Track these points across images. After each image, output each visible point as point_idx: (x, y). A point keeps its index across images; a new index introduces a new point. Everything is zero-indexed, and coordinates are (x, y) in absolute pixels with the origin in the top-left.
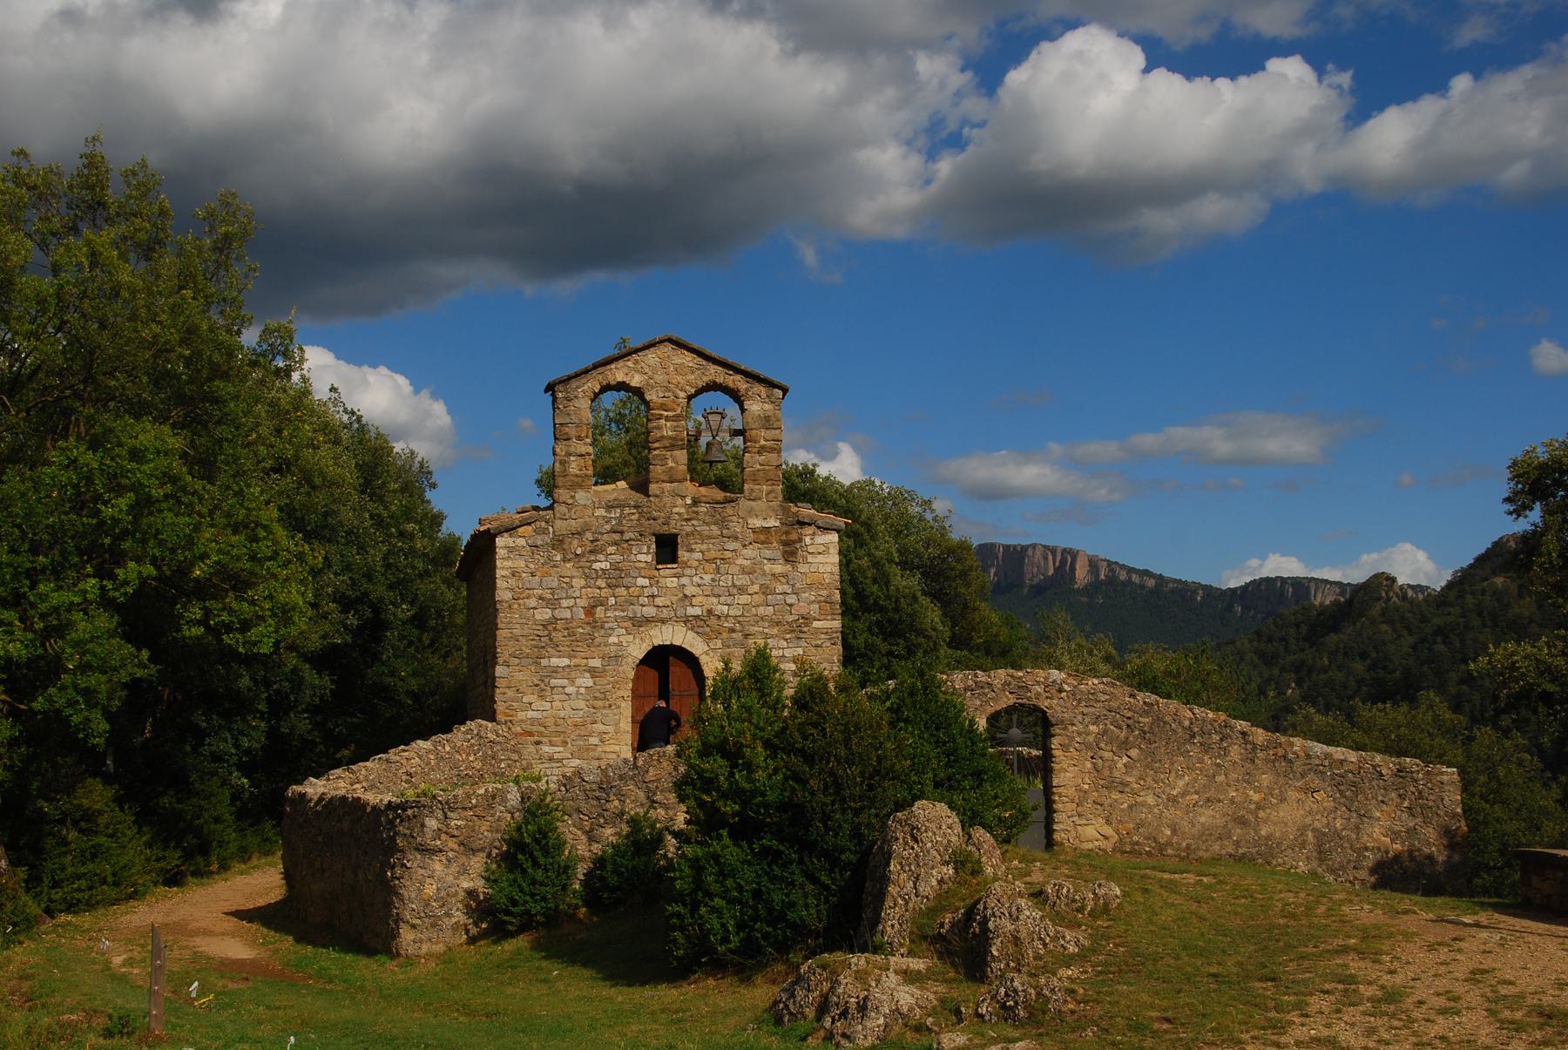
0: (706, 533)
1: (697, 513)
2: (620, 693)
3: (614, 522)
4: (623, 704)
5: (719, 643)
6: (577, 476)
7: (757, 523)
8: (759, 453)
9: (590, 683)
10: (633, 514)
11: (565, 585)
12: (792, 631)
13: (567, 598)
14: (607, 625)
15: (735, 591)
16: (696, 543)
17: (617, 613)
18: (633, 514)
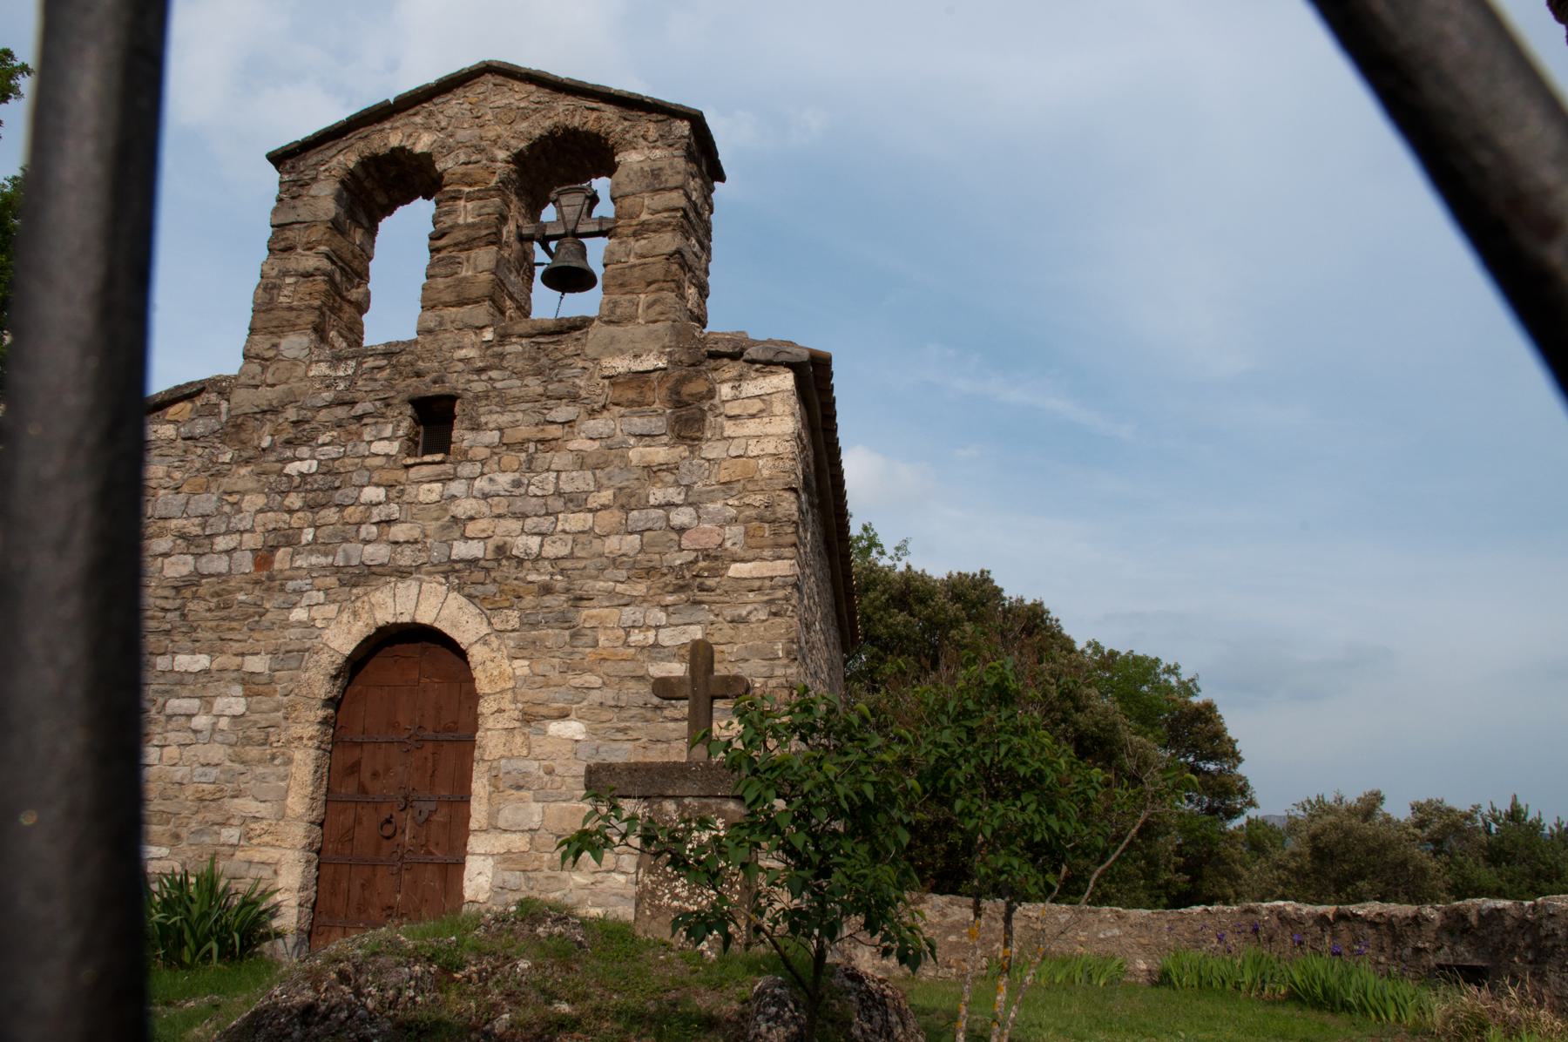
0: (516, 392)
1: (502, 356)
2: (296, 730)
3: (342, 386)
4: (298, 755)
5: (514, 618)
6: (291, 309)
7: (621, 365)
8: (635, 234)
9: (239, 706)
10: (381, 368)
11: (227, 508)
12: (680, 589)
13: (228, 532)
14: (290, 585)
15: (558, 504)
16: (491, 412)
17: (314, 560)
18: (381, 368)
